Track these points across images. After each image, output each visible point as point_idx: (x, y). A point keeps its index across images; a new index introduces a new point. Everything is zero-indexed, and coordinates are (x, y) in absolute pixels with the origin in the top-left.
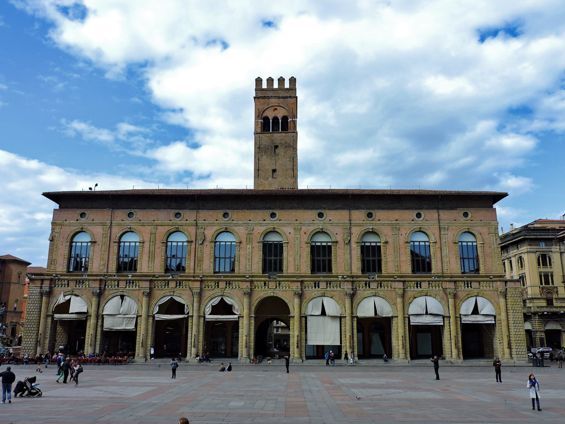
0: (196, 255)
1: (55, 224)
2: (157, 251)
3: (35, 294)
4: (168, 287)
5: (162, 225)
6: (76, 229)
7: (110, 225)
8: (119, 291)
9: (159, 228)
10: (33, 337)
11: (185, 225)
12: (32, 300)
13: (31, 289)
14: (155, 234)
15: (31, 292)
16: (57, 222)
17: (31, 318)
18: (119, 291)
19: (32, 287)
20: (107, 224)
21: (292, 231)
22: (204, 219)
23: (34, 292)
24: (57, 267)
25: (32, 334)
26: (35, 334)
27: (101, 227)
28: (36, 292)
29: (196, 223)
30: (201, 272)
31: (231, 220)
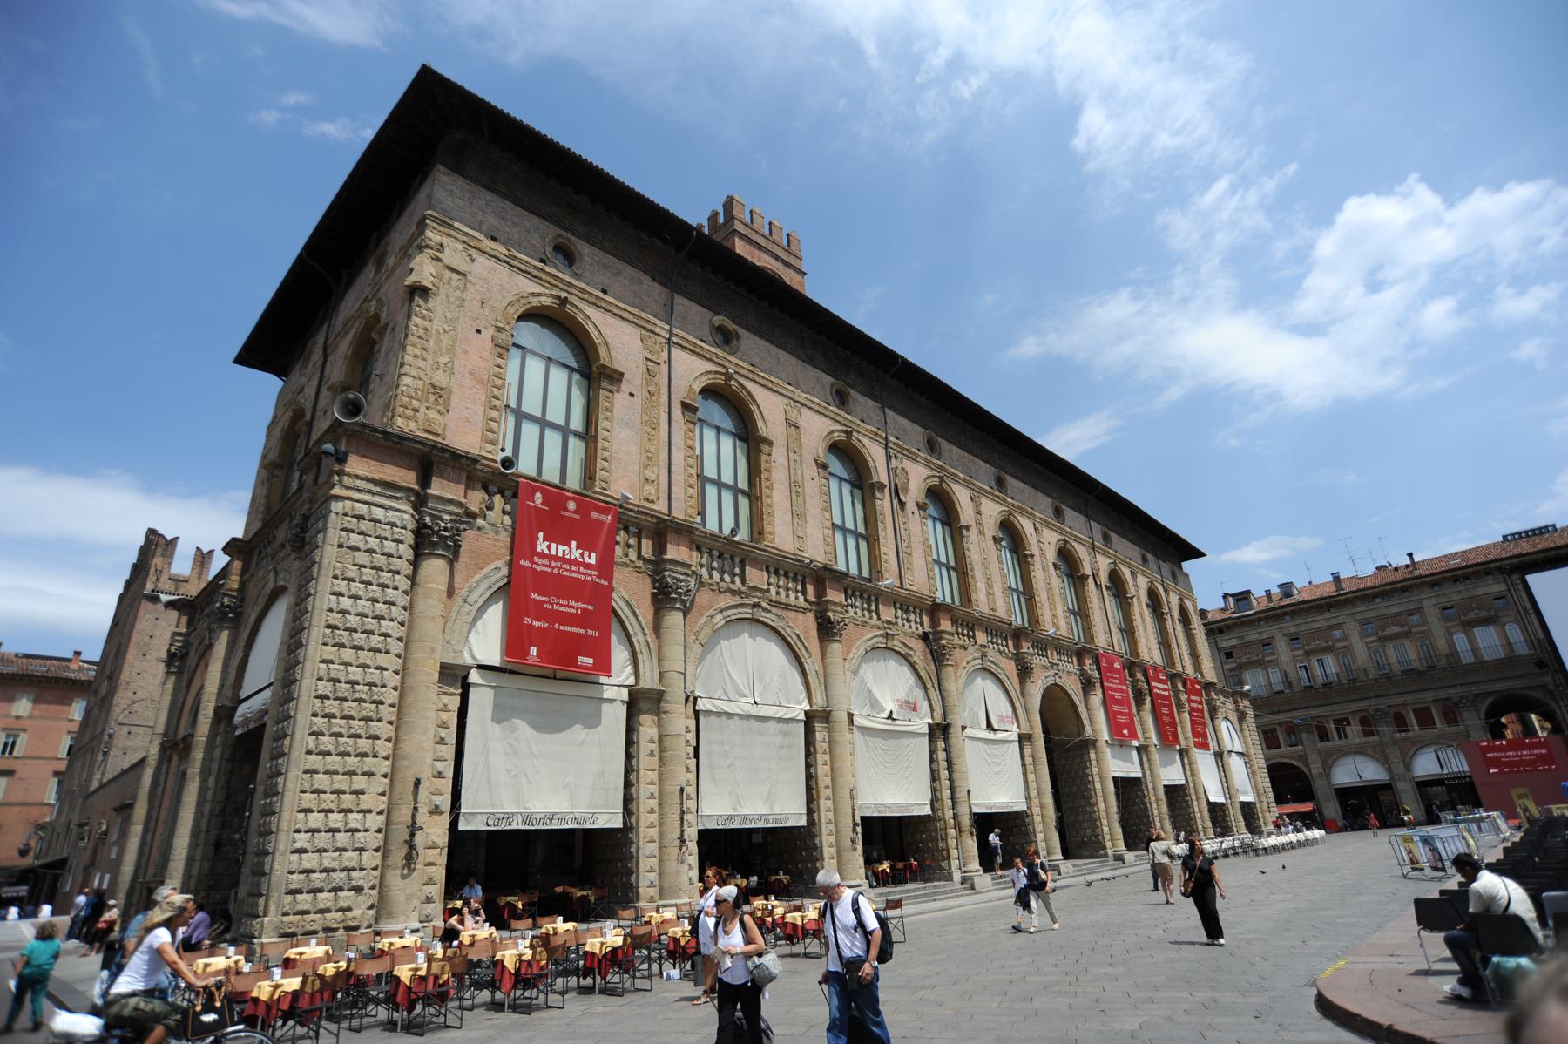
2: (808, 483)
3: (385, 530)
4: (879, 619)
6: (539, 295)
8: (747, 601)
9: (804, 410)
10: (366, 801)
12: (362, 557)
13: (357, 496)
15: (362, 509)
17: (355, 673)
18: (747, 601)
19: (358, 483)
21: (1033, 531)
23: (379, 513)
24: (451, 425)
25: (360, 782)
26: (381, 784)
27: (631, 329)
28: (392, 516)
30: (914, 589)
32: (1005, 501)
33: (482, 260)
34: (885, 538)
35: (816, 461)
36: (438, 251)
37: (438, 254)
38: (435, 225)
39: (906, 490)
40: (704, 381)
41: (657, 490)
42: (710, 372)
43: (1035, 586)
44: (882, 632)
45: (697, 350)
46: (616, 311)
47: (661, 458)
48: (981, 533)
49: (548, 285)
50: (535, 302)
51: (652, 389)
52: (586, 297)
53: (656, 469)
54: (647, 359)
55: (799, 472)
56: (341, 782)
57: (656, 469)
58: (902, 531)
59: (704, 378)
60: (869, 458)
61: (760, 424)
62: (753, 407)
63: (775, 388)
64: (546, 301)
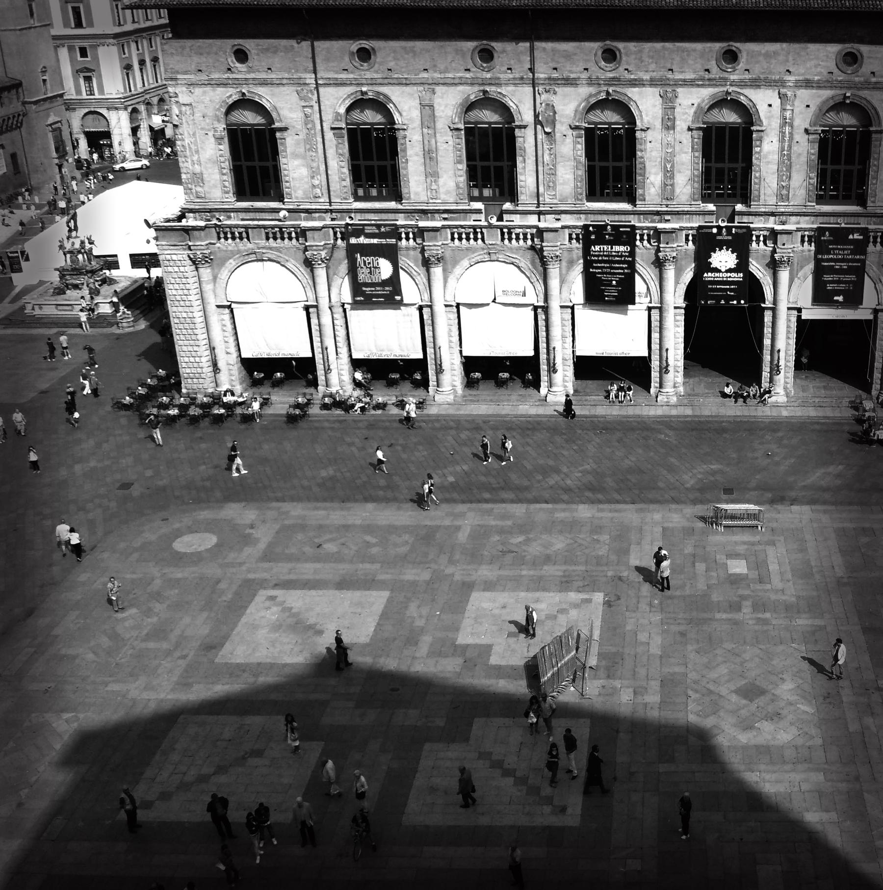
0: (540, 159)
1: (173, 83)
2: (442, 147)
5: (448, 82)
6: (231, 96)
7: (314, 82)
9: (438, 89)
11: (506, 82)
14: (431, 106)
16: (179, 76)
20: (307, 82)
21: (777, 102)
22: (555, 66)
29: (533, 79)
31: (621, 69)
32: (726, 79)
33: (198, 91)
34: (524, 168)
35: (450, 127)
36: (176, 97)
37: (176, 99)
38: (170, 82)
39: (553, 123)
40: (348, 103)
41: (321, 190)
42: (352, 94)
43: (754, 161)
44: (485, 251)
45: (339, 82)
46: (278, 82)
47: (321, 169)
48: (669, 124)
49: (235, 86)
50: (230, 101)
51: (309, 126)
52: (257, 82)
53: (319, 177)
54: (304, 107)
55: (433, 141)
56: (190, 348)
57: (319, 177)
58: (547, 158)
59: (347, 102)
60: (511, 104)
61: (396, 116)
62: (390, 106)
63: (408, 82)
64: (236, 97)
